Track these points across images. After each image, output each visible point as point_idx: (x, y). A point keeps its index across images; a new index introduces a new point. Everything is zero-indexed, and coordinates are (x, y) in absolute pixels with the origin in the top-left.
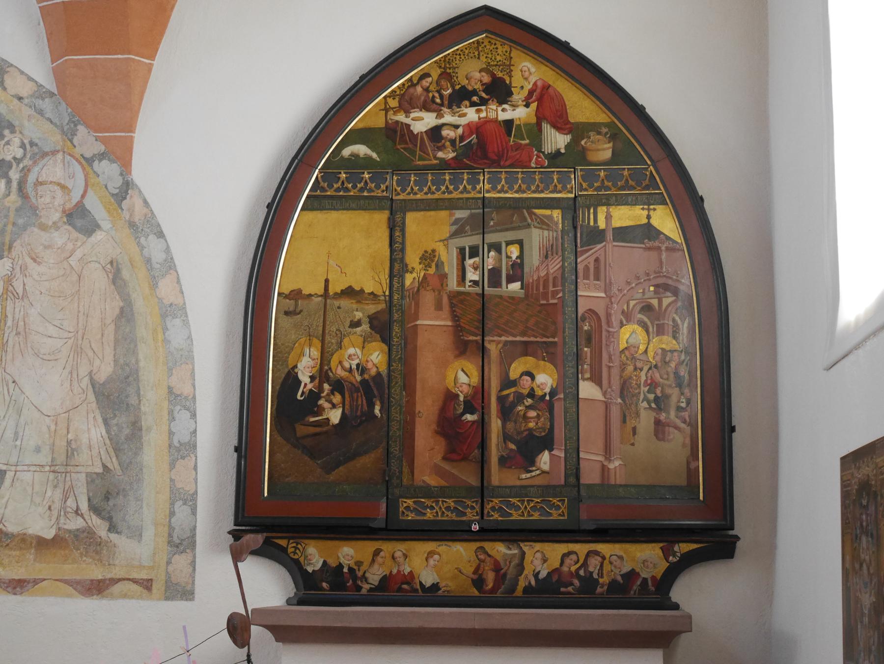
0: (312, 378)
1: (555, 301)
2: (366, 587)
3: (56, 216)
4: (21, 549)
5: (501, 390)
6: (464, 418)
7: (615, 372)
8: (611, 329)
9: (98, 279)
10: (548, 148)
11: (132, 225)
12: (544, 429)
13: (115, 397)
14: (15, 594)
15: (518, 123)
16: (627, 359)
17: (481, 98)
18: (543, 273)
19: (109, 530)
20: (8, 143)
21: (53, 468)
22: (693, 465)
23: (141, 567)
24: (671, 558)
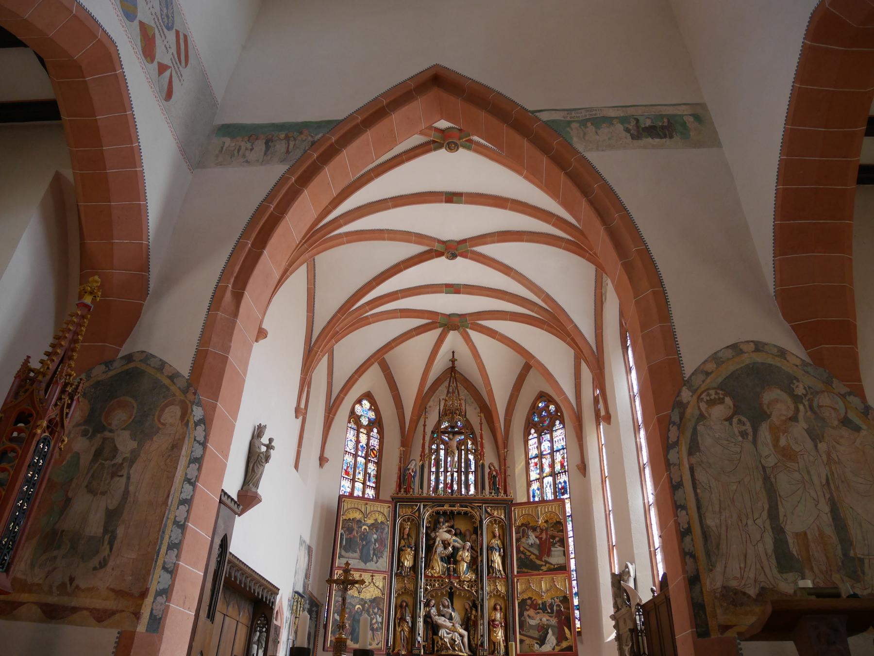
3: (836, 423)
20: (797, 387)
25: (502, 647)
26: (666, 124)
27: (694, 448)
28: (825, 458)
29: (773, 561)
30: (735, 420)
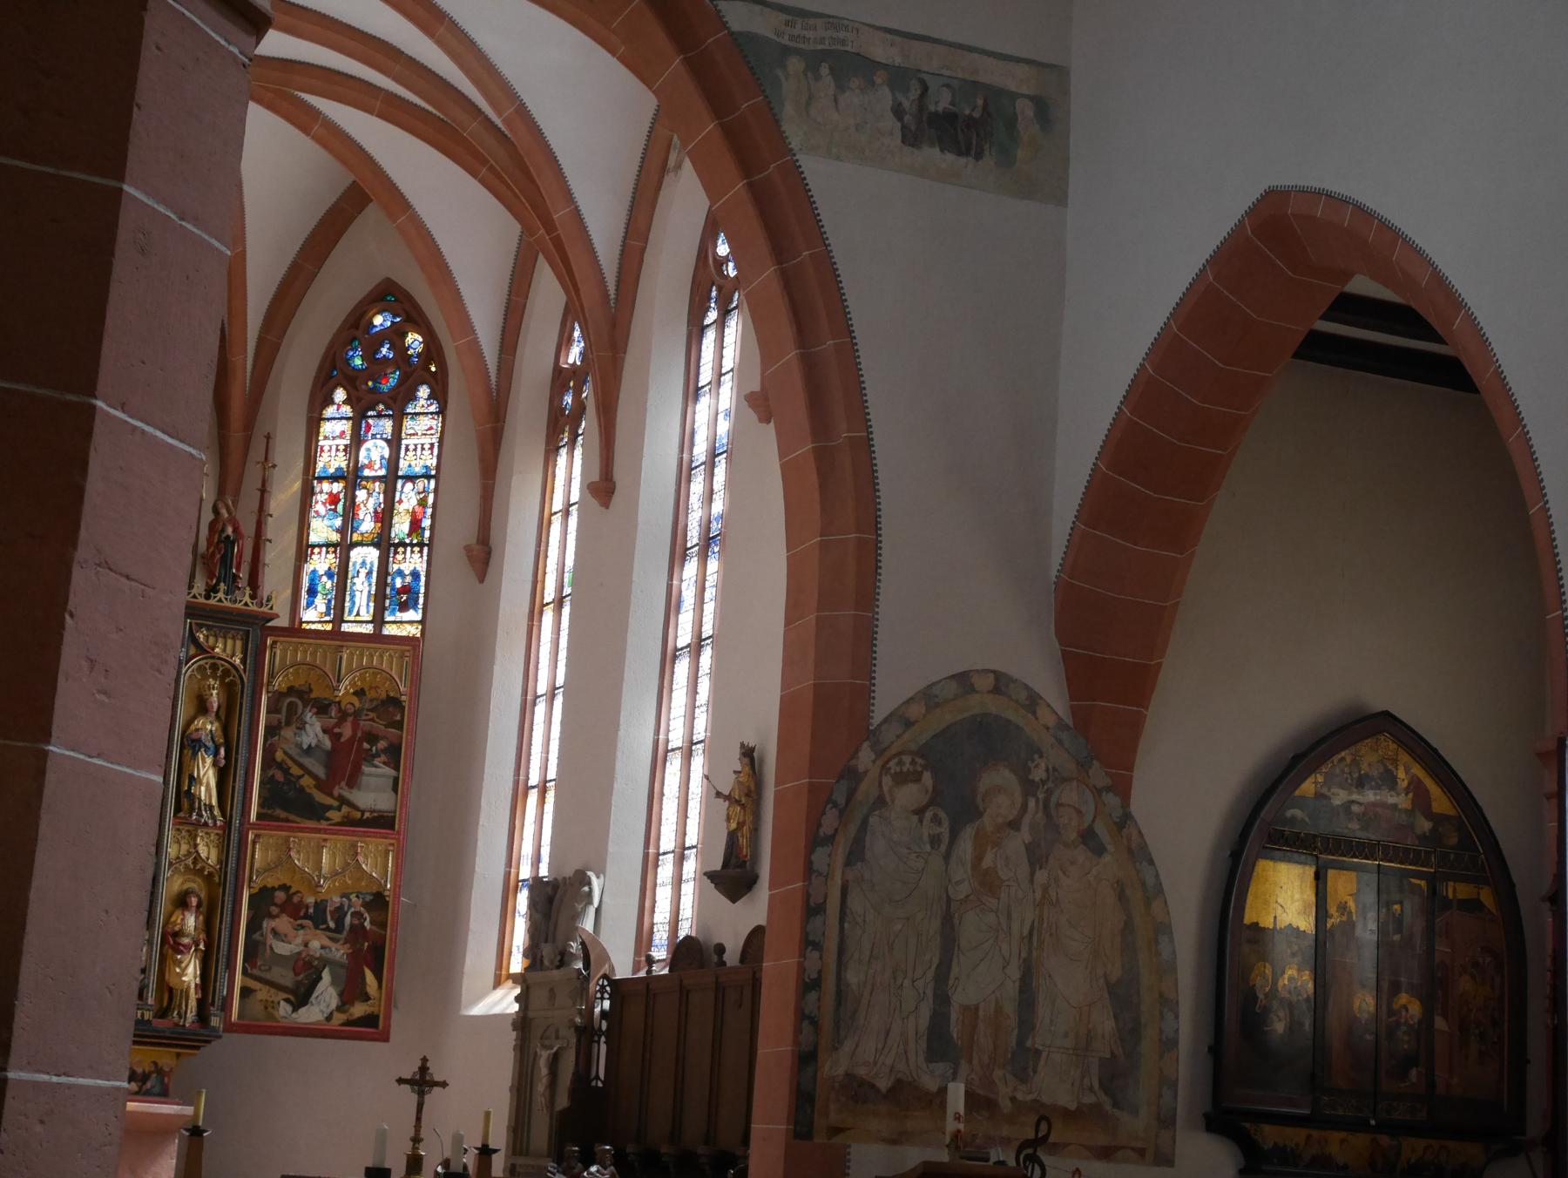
3: (1073, 836)
11: (1130, 851)
13: (1122, 995)
25: (193, 1003)
26: (977, 115)
27: (856, 854)
28: (1038, 895)
29: (923, 1045)
30: (929, 815)
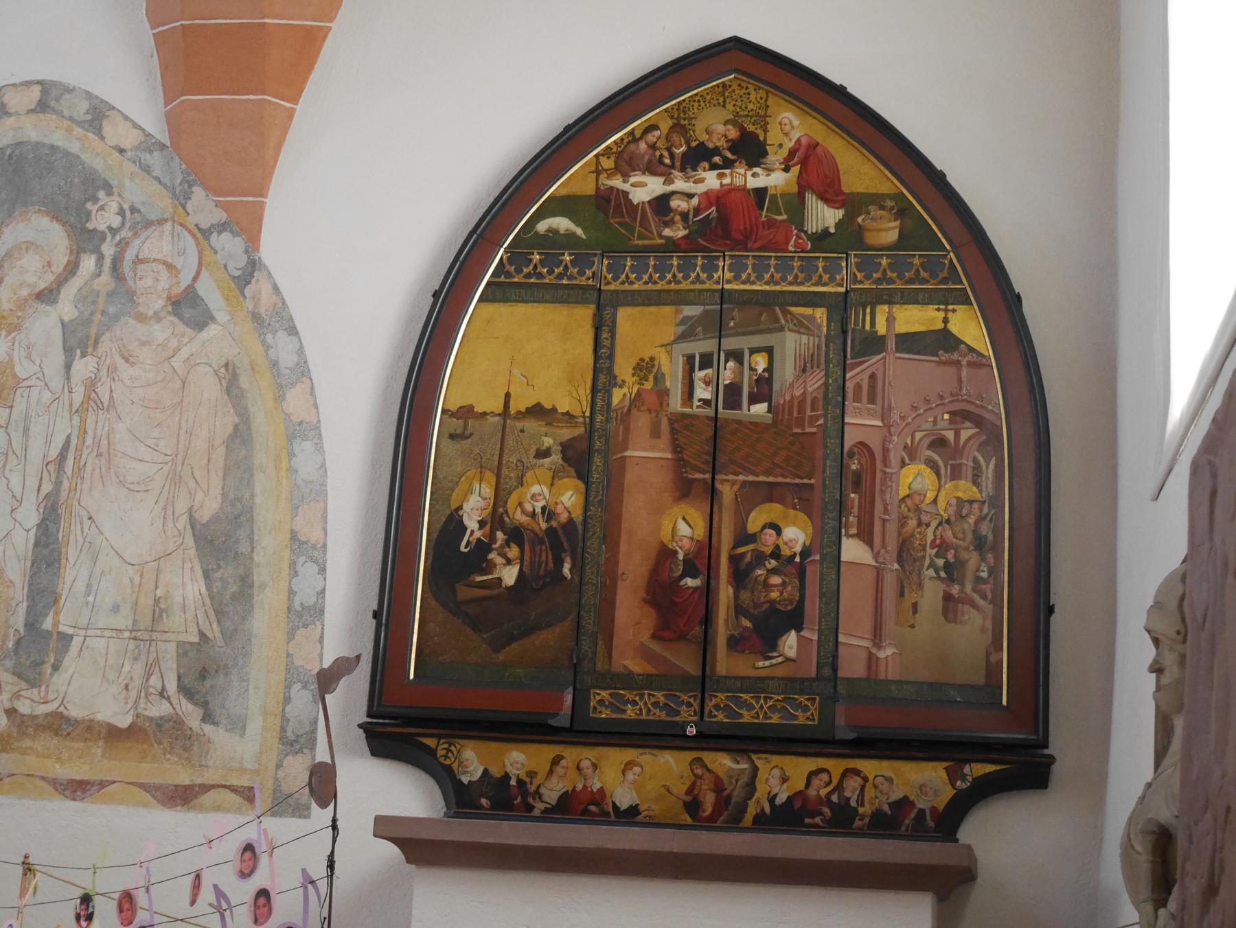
0: (482, 524)
1: (813, 430)
2: (539, 806)
3: (159, 304)
4: (86, 740)
5: (735, 547)
6: (682, 583)
7: (892, 527)
8: (888, 470)
9: (208, 387)
10: (813, 226)
11: (256, 317)
12: (790, 601)
13: (220, 544)
14: (74, 799)
15: (773, 192)
16: (909, 510)
17: (725, 159)
18: (798, 393)
19: (203, 720)
20: (102, 208)
21: (134, 634)
22: (993, 659)
23: (243, 771)
24: (959, 783)
28: (78, 398)
